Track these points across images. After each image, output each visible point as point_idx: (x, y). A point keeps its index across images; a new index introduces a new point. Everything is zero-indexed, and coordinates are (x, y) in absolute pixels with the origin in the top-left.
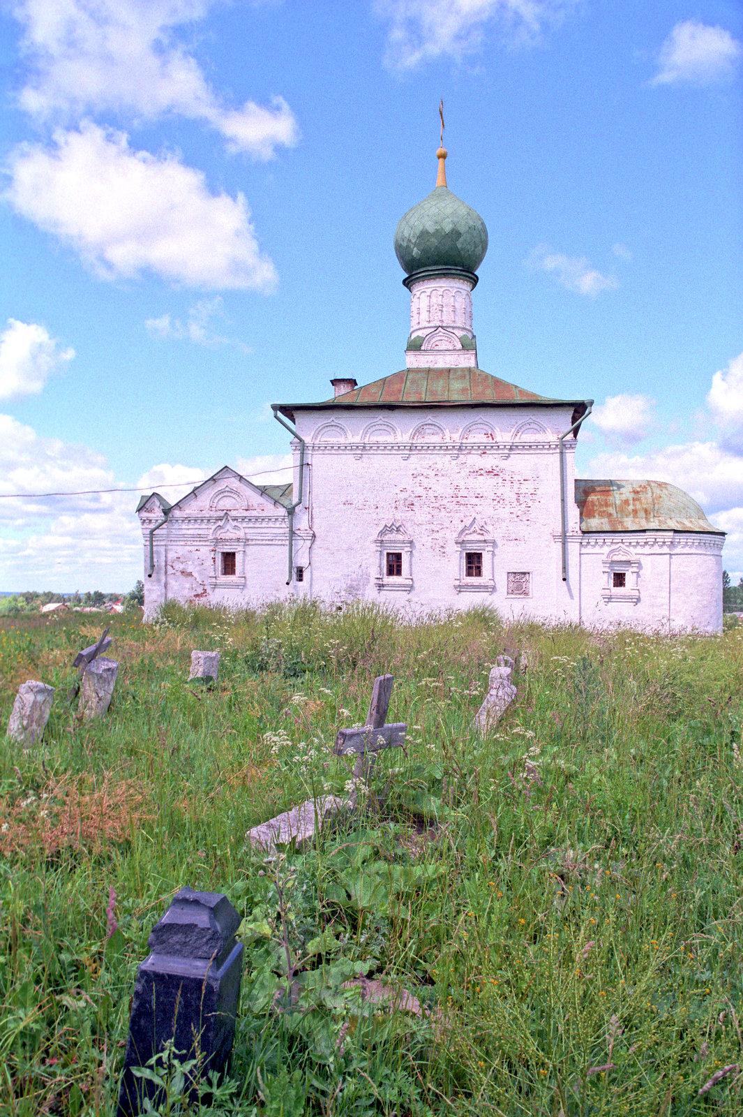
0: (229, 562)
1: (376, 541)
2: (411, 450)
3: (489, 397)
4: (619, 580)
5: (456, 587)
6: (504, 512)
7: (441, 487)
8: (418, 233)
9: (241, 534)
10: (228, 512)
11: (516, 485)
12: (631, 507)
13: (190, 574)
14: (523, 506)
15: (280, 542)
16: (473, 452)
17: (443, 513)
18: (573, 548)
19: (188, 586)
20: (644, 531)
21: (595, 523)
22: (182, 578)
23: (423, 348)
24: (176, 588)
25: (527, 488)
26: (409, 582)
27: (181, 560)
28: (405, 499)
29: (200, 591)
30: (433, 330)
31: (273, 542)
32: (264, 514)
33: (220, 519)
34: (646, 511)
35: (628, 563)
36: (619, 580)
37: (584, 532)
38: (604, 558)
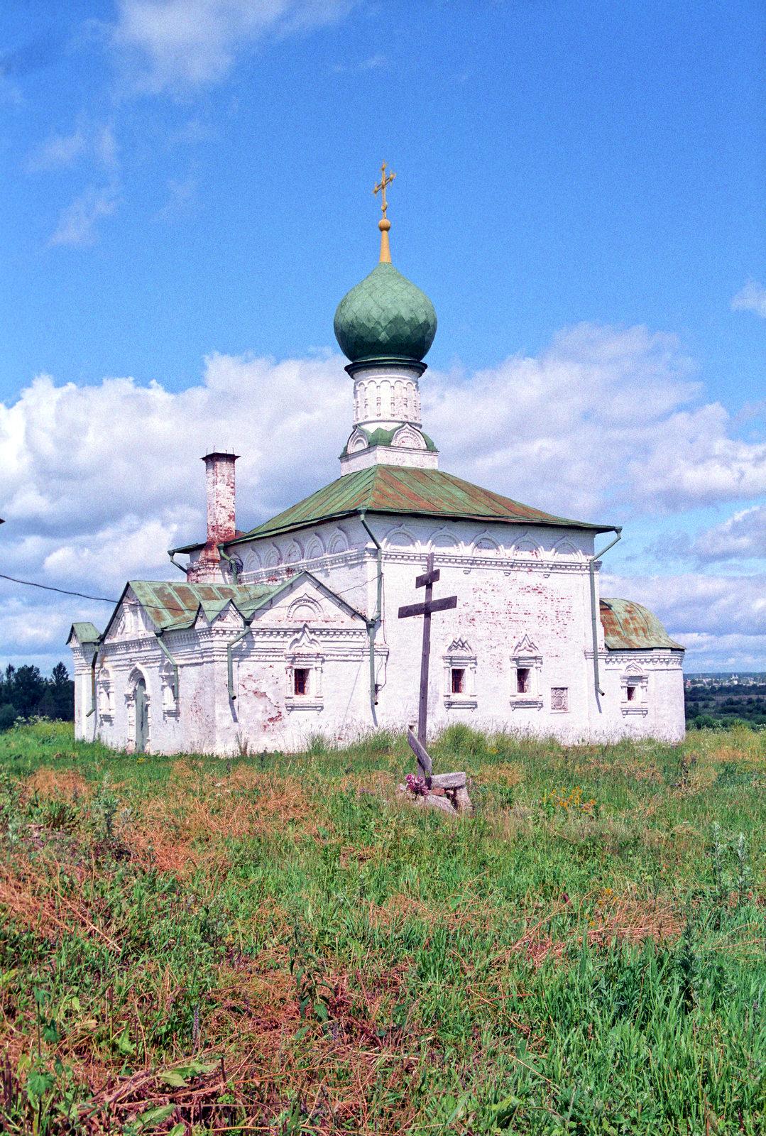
1: (444, 658)
2: (471, 564)
4: (630, 691)
5: (512, 704)
6: (547, 630)
7: (497, 603)
8: (391, 317)
9: (316, 649)
10: (308, 624)
11: (555, 603)
12: (632, 626)
13: (264, 695)
14: (561, 623)
15: (355, 658)
16: (522, 569)
17: (499, 629)
18: (601, 662)
19: (261, 708)
20: (652, 649)
21: (614, 641)
22: (255, 699)
23: (392, 444)
24: (248, 711)
25: (563, 606)
27: (253, 678)
28: (468, 614)
29: (274, 714)
30: (401, 424)
31: (349, 658)
32: (344, 627)
33: (297, 631)
34: (643, 630)
35: (640, 678)
36: (630, 691)
37: (609, 650)
38: (623, 673)
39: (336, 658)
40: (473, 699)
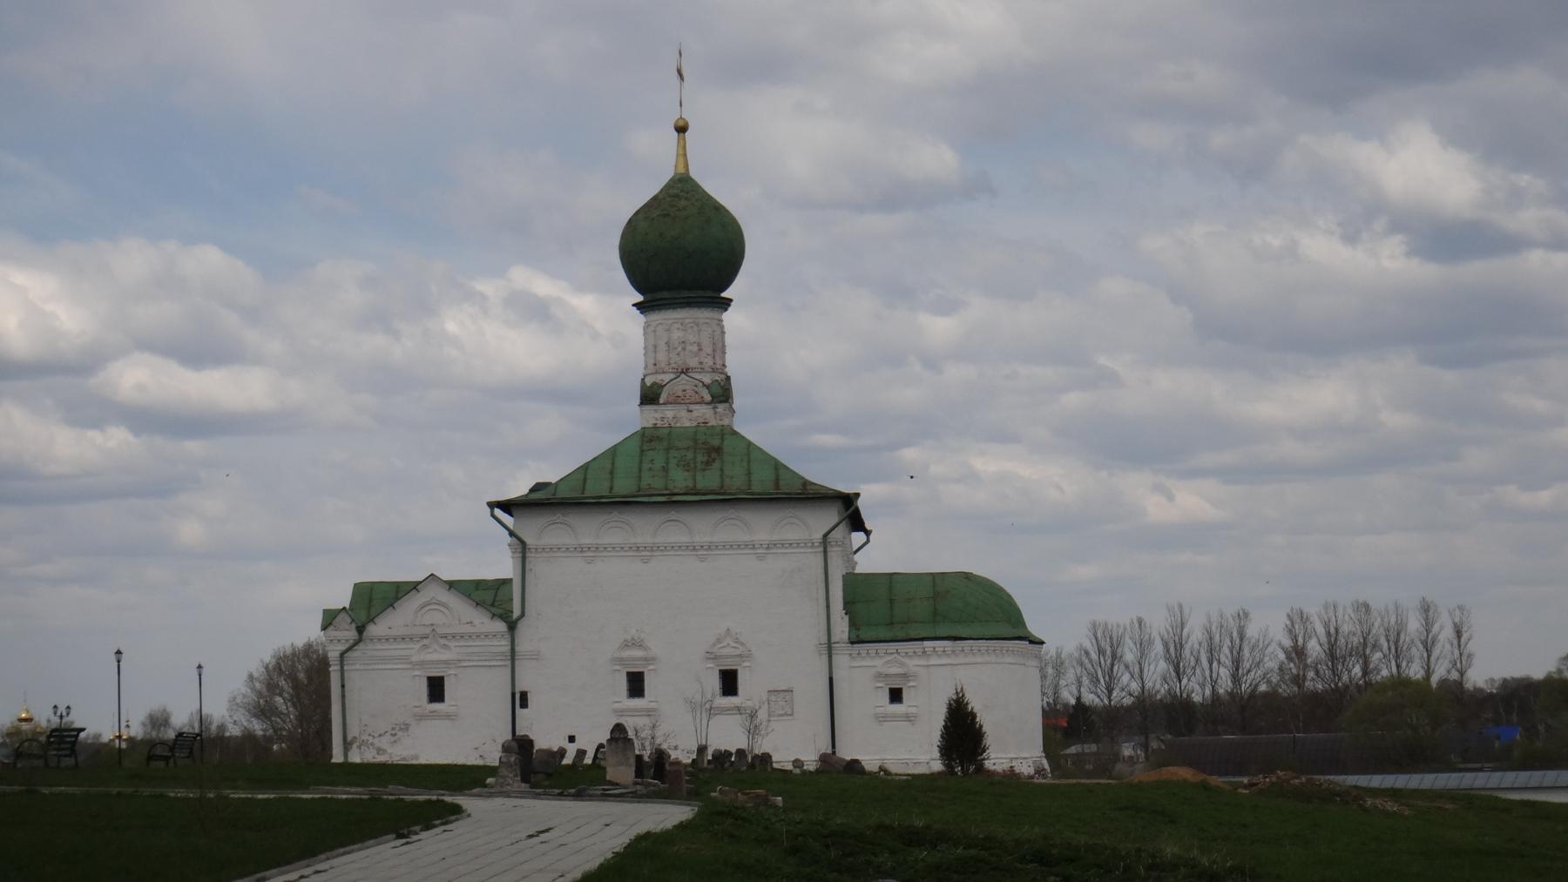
0: (436, 689)
4: (896, 695)
18: (842, 660)
26: (653, 705)
36: (896, 695)
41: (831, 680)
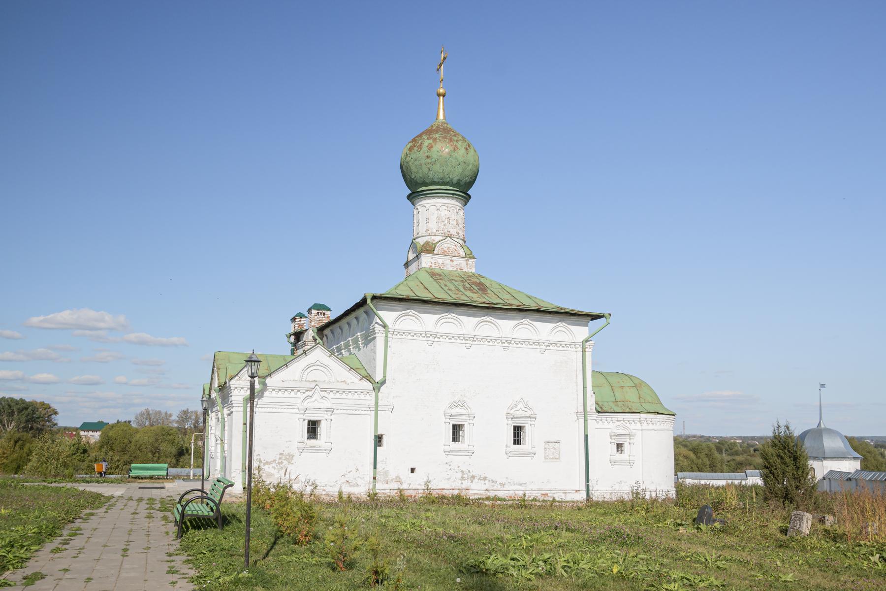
0: (313, 428)
3: (476, 298)
9: (326, 404)
18: (590, 423)
23: (435, 252)
30: (441, 238)
31: (359, 412)
36: (619, 446)
39: (345, 412)
40: (471, 448)
41: (586, 437)
